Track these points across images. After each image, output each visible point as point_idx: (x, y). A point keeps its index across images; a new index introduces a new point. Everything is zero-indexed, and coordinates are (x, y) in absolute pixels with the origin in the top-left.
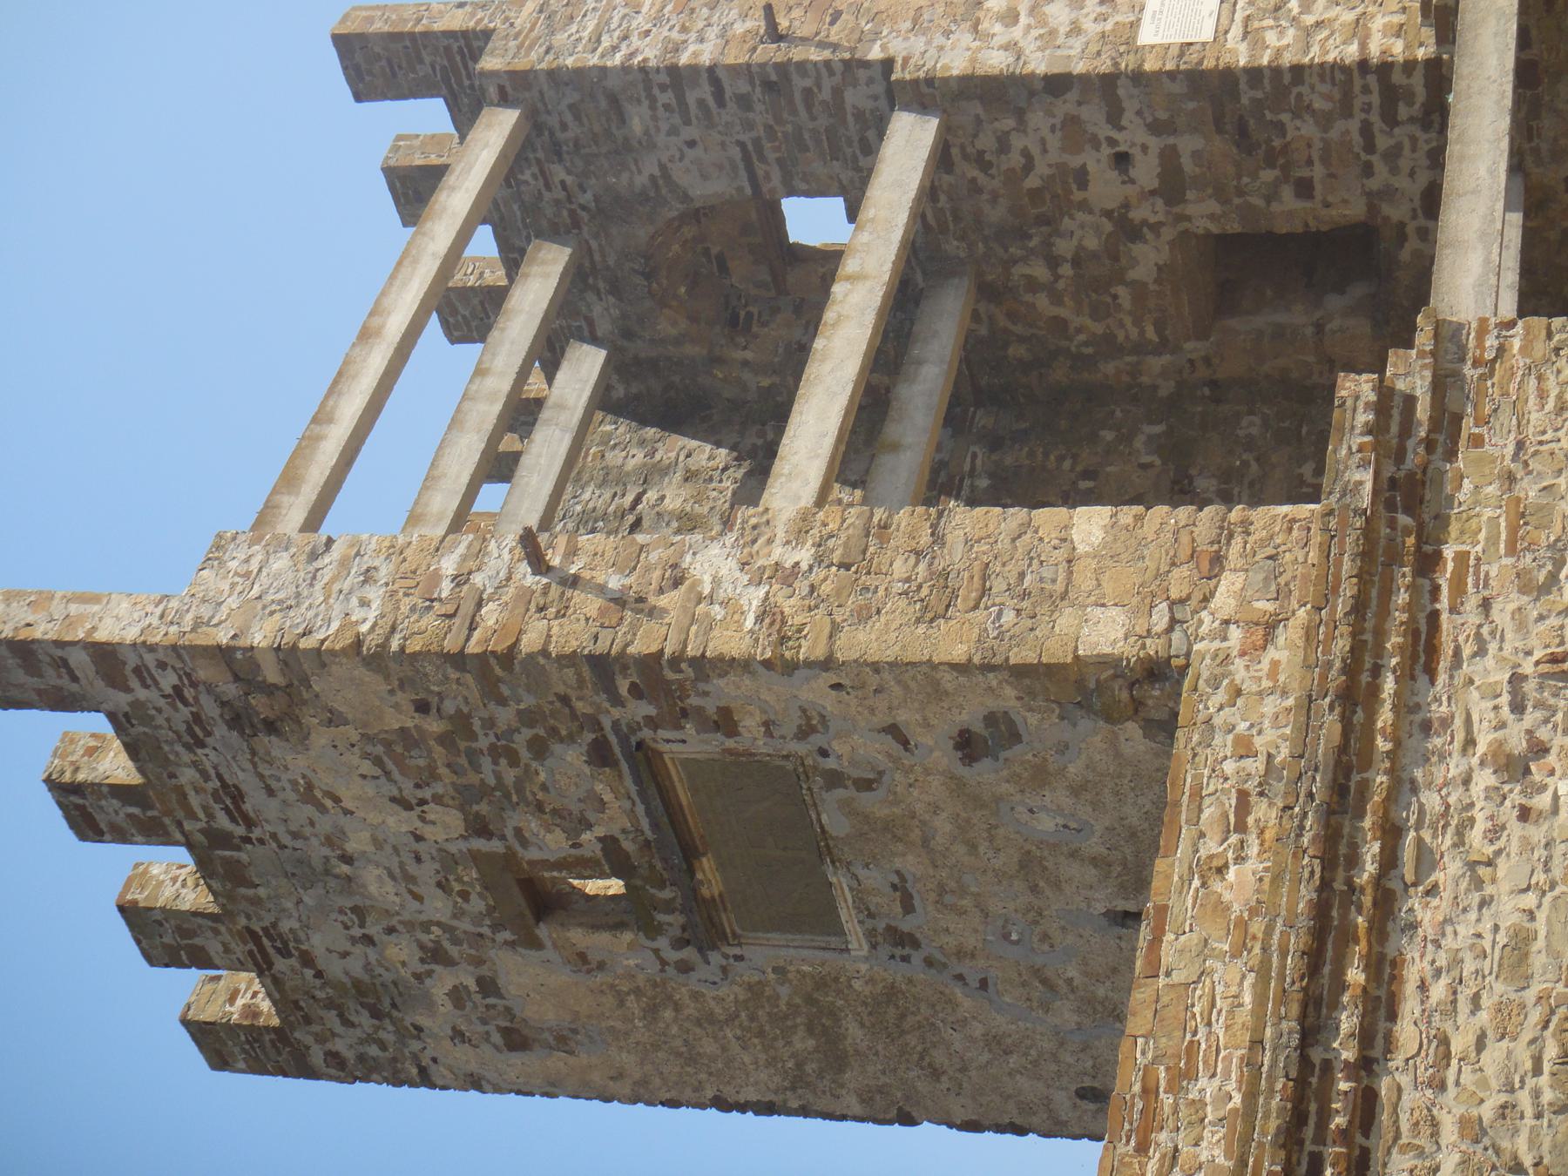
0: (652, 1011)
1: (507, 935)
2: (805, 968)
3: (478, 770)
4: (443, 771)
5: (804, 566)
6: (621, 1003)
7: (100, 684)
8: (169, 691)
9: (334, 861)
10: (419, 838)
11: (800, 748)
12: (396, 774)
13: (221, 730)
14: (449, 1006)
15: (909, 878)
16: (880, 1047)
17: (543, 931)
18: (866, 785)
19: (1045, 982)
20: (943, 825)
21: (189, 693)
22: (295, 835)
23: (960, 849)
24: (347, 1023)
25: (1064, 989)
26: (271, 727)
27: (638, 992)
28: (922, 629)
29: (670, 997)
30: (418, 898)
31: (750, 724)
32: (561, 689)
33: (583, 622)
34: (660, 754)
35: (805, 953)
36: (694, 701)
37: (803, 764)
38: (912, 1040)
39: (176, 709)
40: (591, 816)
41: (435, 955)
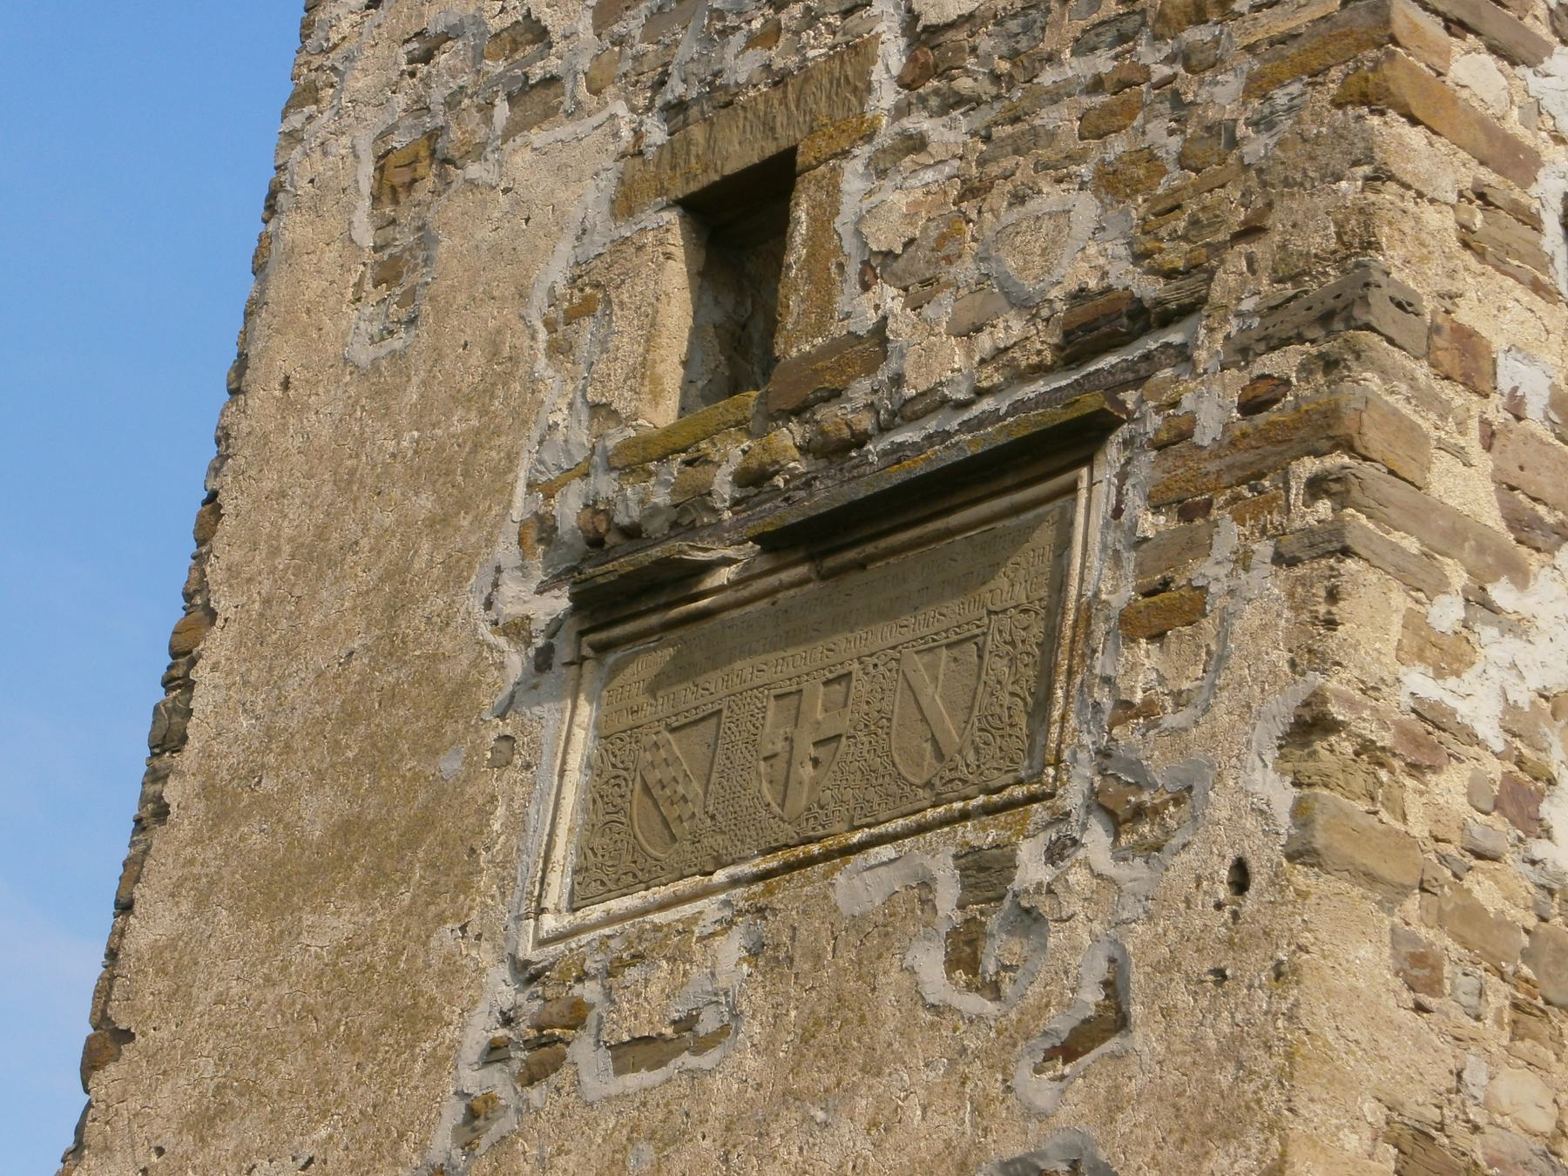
5: (1540, 849)
6: (458, 399)
15: (707, 1061)
16: (285, 990)
28: (1372, 1111)
29: (464, 505)
33: (1447, 285)
34: (1088, 461)
36: (1229, 533)
37: (1032, 799)
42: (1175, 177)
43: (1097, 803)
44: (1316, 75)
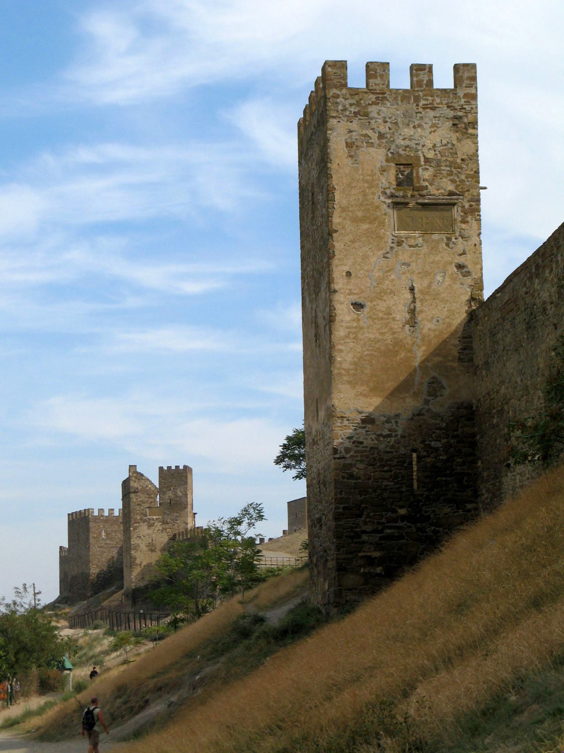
0: (367, 182)
1: (390, 155)
2: (387, 221)
3: (446, 166)
4: (445, 158)
6: (369, 175)
7: (466, 92)
8: (464, 107)
9: (414, 124)
10: (423, 146)
11: (457, 234)
12: (442, 148)
13: (451, 114)
14: (362, 133)
17: (393, 165)
18: (447, 245)
19: (389, 271)
20: (438, 258)
21: (463, 111)
22: (421, 118)
23: (431, 260)
24: (351, 105)
25: (387, 274)
26: (454, 125)
27: (373, 180)
30: (404, 139)
31: (463, 226)
32: (471, 191)
35: (392, 221)
36: (470, 217)
38: (364, 239)
39: (459, 106)
40: (433, 186)
41: (381, 136)
42: (458, 183)
43: (460, 235)
44: (473, 179)
